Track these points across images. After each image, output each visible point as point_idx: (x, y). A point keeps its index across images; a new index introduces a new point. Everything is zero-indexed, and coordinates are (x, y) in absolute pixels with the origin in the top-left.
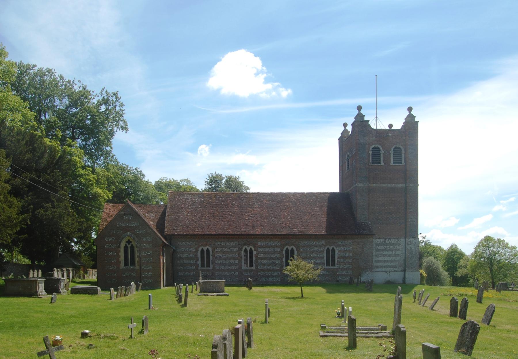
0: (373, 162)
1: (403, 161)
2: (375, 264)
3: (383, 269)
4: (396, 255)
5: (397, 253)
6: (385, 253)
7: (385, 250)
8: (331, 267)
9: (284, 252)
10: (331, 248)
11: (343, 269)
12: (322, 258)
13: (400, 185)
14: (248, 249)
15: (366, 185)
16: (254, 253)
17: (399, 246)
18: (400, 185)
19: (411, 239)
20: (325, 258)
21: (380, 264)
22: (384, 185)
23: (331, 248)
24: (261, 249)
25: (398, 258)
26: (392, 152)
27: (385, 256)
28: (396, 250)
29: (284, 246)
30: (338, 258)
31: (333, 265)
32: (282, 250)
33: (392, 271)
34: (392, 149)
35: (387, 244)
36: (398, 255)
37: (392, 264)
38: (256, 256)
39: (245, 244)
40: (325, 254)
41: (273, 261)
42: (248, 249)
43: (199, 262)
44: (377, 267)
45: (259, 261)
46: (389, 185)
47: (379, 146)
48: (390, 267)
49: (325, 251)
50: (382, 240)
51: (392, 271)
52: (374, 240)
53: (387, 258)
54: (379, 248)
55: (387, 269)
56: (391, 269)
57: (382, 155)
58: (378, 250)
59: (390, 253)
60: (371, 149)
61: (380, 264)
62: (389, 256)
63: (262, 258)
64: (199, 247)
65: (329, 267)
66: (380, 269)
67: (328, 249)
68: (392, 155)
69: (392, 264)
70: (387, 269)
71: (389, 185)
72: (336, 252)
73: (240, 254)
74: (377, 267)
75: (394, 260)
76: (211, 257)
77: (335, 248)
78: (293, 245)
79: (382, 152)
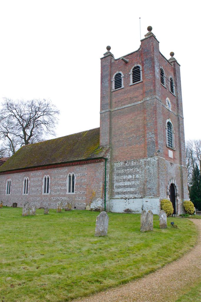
0: (116, 88)
1: (141, 78)
2: (116, 190)
3: (123, 196)
4: (136, 179)
5: (137, 176)
6: (125, 177)
7: (125, 174)
8: (71, 193)
9: (44, 180)
10: (71, 175)
11: (79, 196)
12: (65, 186)
13: (140, 102)
14: (26, 179)
15: (107, 110)
16: (29, 181)
17: (139, 168)
18: (140, 102)
19: (149, 159)
20: (68, 185)
21: (120, 190)
22: (124, 107)
23: (71, 175)
24: (32, 179)
25: (138, 183)
26: (131, 72)
27: (124, 180)
28: (136, 173)
29: (44, 175)
30: (76, 184)
31: (73, 191)
32: (42, 179)
33: (131, 198)
34: (131, 70)
35: (127, 168)
36: (138, 179)
37: (132, 190)
38: (30, 185)
39: (25, 176)
40: (68, 181)
41: (38, 188)
42: (26, 179)
43: (6, 191)
44: (118, 193)
45: (31, 188)
46: (130, 105)
47: (121, 72)
48: (131, 193)
49: (68, 178)
50: (122, 163)
51: (131, 198)
52: (115, 164)
53: (127, 183)
54: (120, 172)
55: (127, 196)
56: (131, 196)
57: (122, 79)
58: (118, 175)
59: (130, 176)
60: (114, 77)
61: (120, 190)
62: (129, 180)
63: (33, 187)
64: (7, 180)
65: (70, 193)
66: (120, 196)
67: (70, 176)
68: (131, 76)
69: (132, 190)
70: (127, 196)
71: (130, 105)
72: (75, 178)
73: (22, 184)
74: (118, 193)
75: (134, 185)
76: (11, 186)
77: (74, 175)
78: (48, 174)
79: (123, 75)
